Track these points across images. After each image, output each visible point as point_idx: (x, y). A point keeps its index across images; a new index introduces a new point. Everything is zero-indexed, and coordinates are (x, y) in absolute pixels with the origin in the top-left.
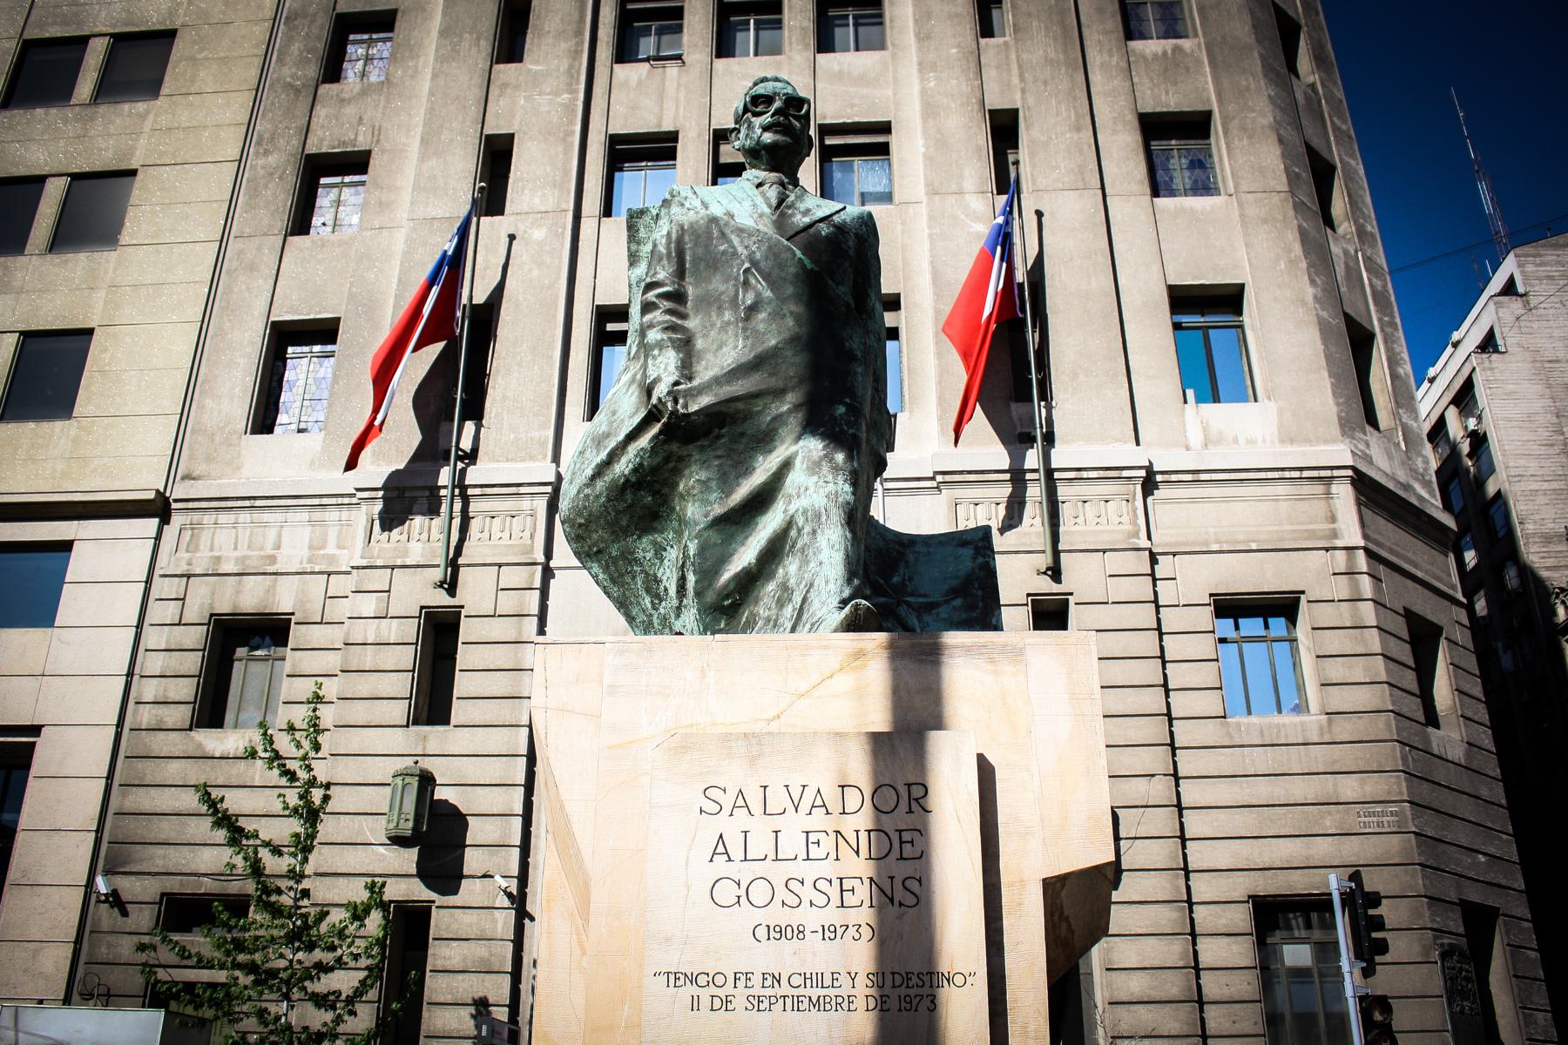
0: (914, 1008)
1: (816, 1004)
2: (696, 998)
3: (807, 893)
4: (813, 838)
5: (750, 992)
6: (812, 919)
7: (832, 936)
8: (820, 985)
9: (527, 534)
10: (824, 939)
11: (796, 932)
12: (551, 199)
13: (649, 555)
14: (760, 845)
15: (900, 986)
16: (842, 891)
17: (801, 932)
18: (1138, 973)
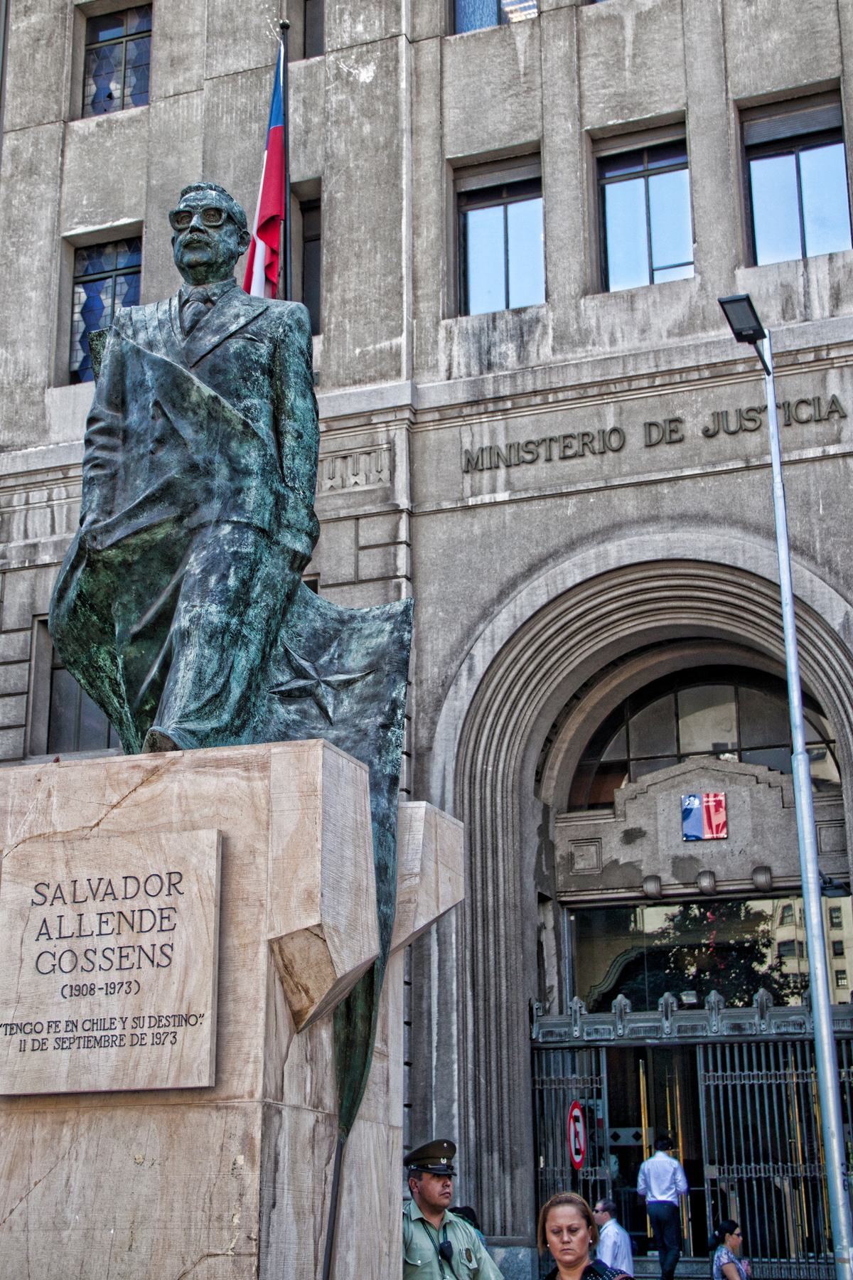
1: (98, 1042)
3: (98, 960)
4: (104, 919)
6: (99, 979)
13: (108, 663)
16: (121, 957)
17: (92, 990)
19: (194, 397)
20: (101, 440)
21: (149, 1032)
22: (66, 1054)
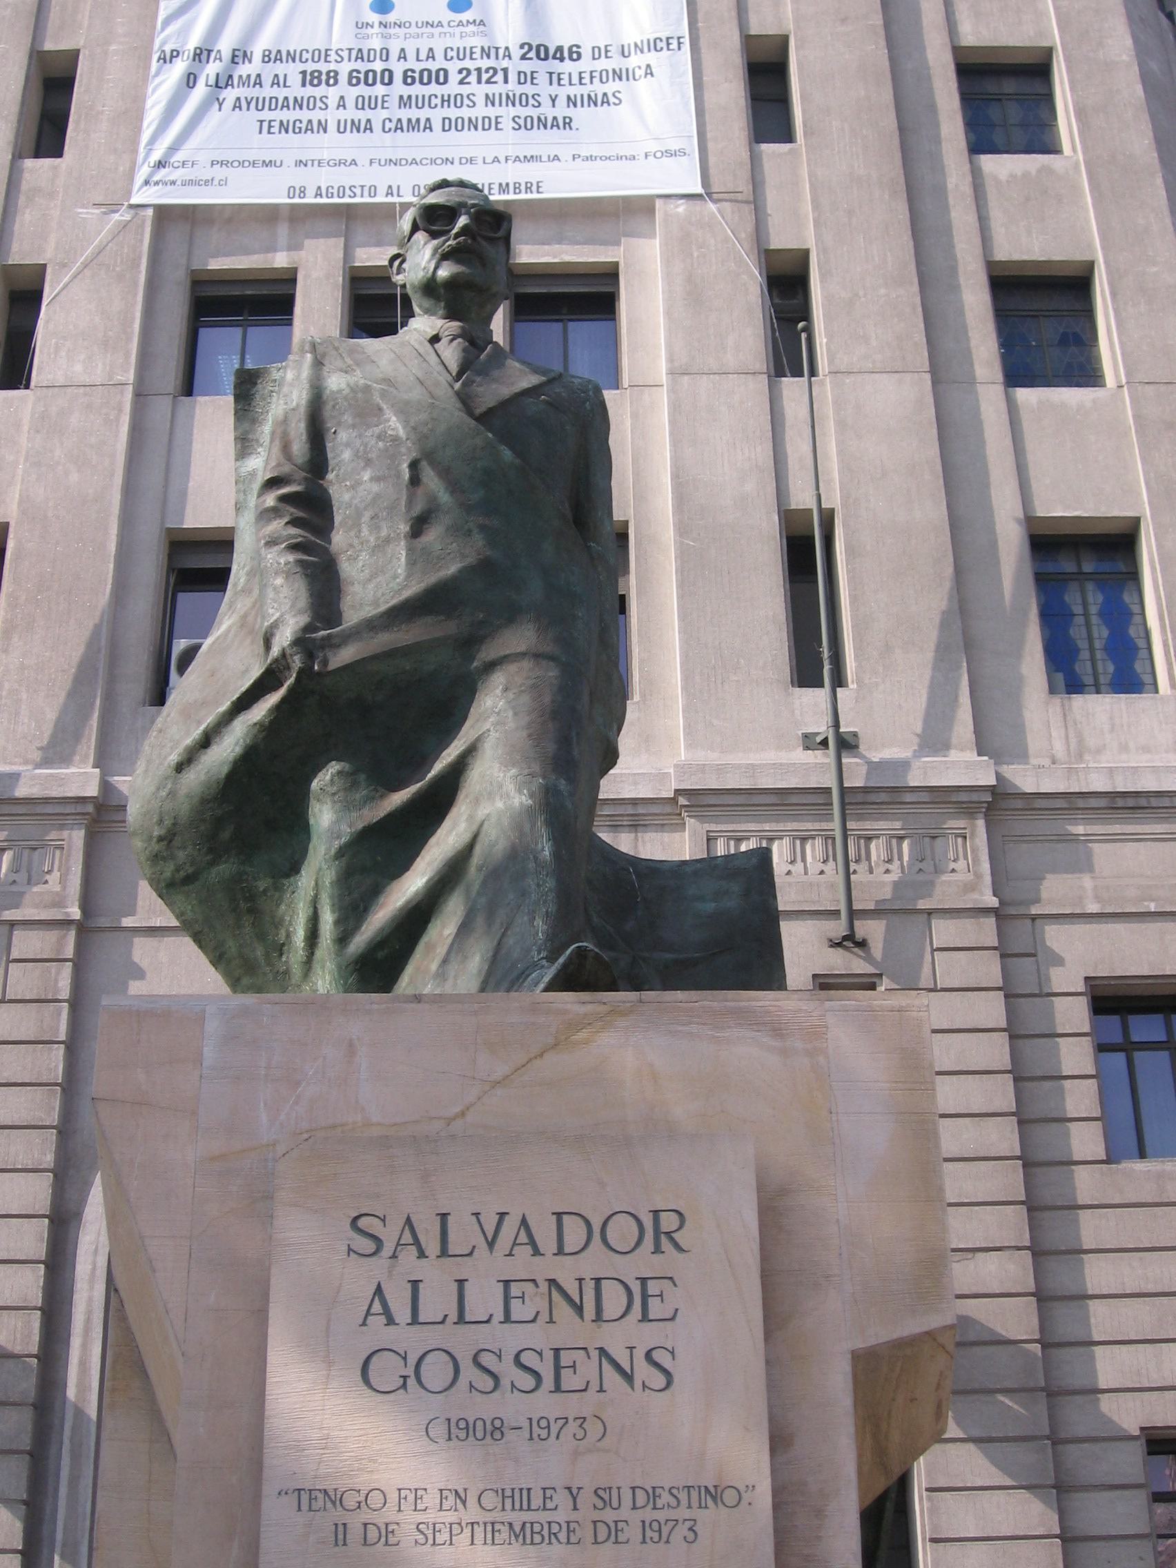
2: (341, 1528)
4: (515, 1290)
5: (420, 1517)
7: (544, 1433)
8: (525, 1507)
10: (531, 1439)
11: (489, 1427)
14: (436, 1302)
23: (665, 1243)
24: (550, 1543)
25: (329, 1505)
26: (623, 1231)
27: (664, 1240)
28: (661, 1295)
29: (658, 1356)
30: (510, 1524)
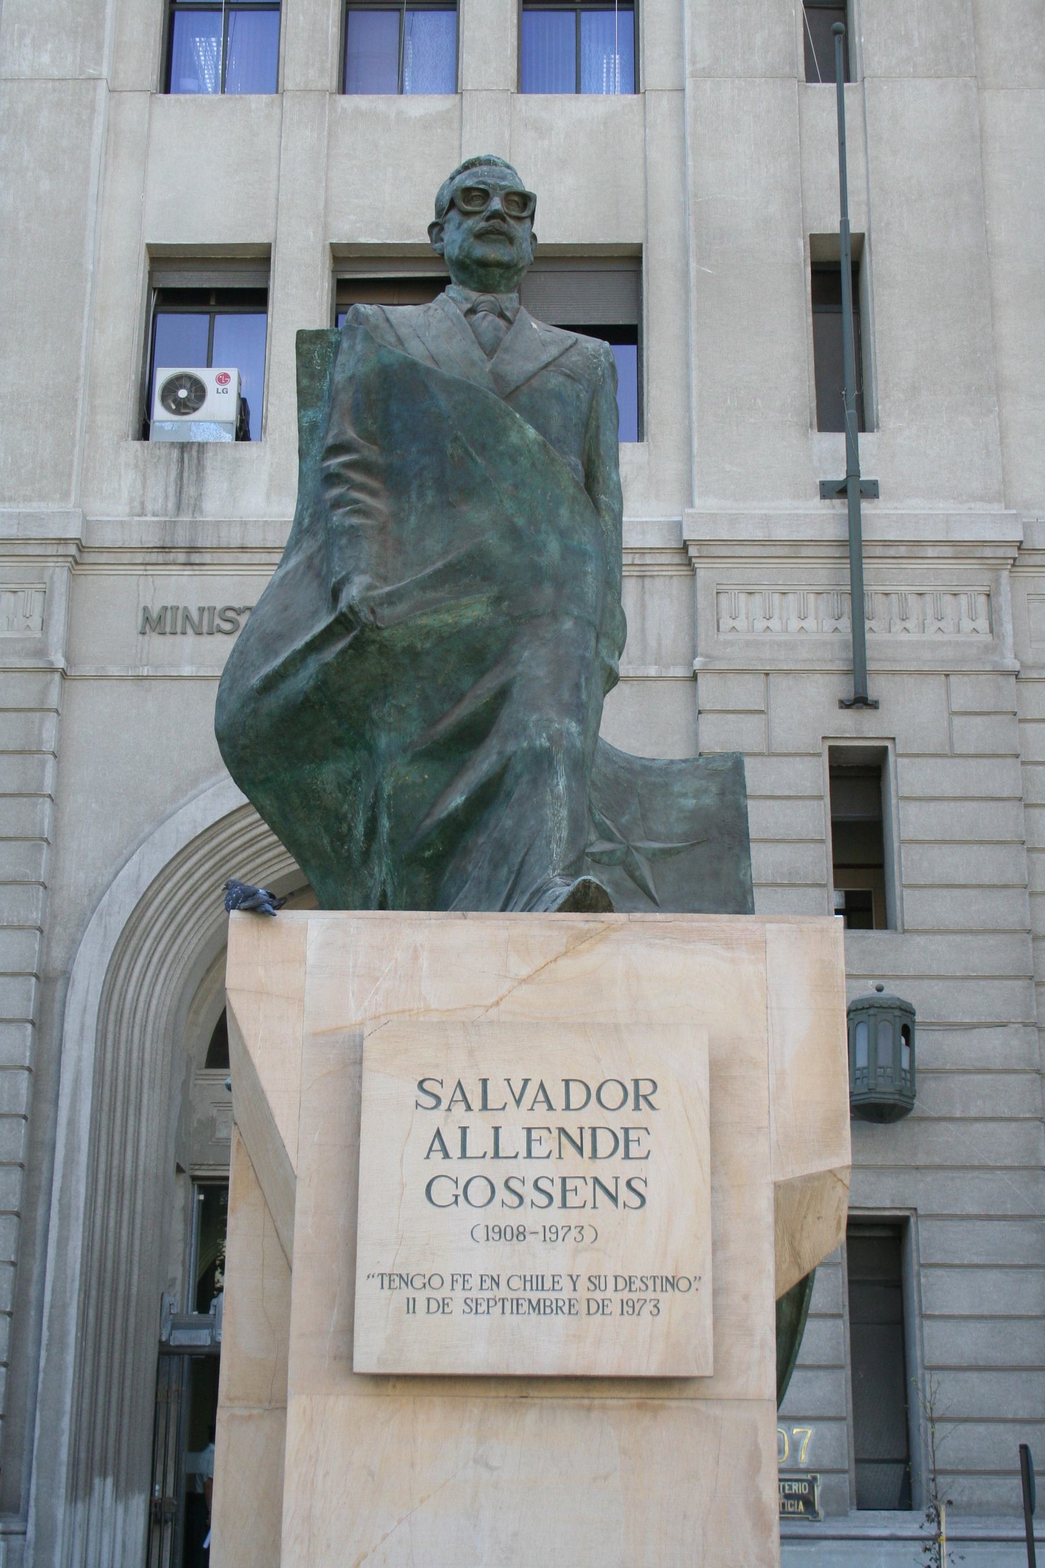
0: (636, 1311)
1: (537, 1307)
3: (529, 1193)
4: (535, 1135)
5: (468, 1294)
8: (540, 1287)
9: (36, 622)
10: (545, 1240)
12: (70, 58)
14: (479, 1142)
15: (623, 1290)
18: (972, 1325)
19: (514, 438)
20: (357, 477)
21: (617, 1297)
22: (483, 1320)
23: (642, 1103)
24: (557, 1313)
25: (403, 1284)
26: (612, 1095)
27: (642, 1101)
28: (638, 1141)
29: (634, 1184)
30: (530, 1301)
